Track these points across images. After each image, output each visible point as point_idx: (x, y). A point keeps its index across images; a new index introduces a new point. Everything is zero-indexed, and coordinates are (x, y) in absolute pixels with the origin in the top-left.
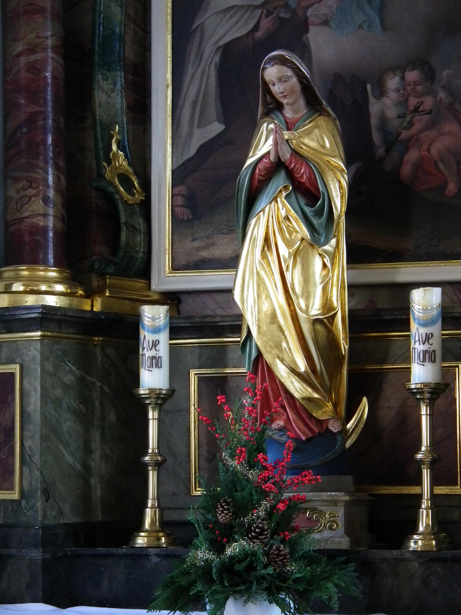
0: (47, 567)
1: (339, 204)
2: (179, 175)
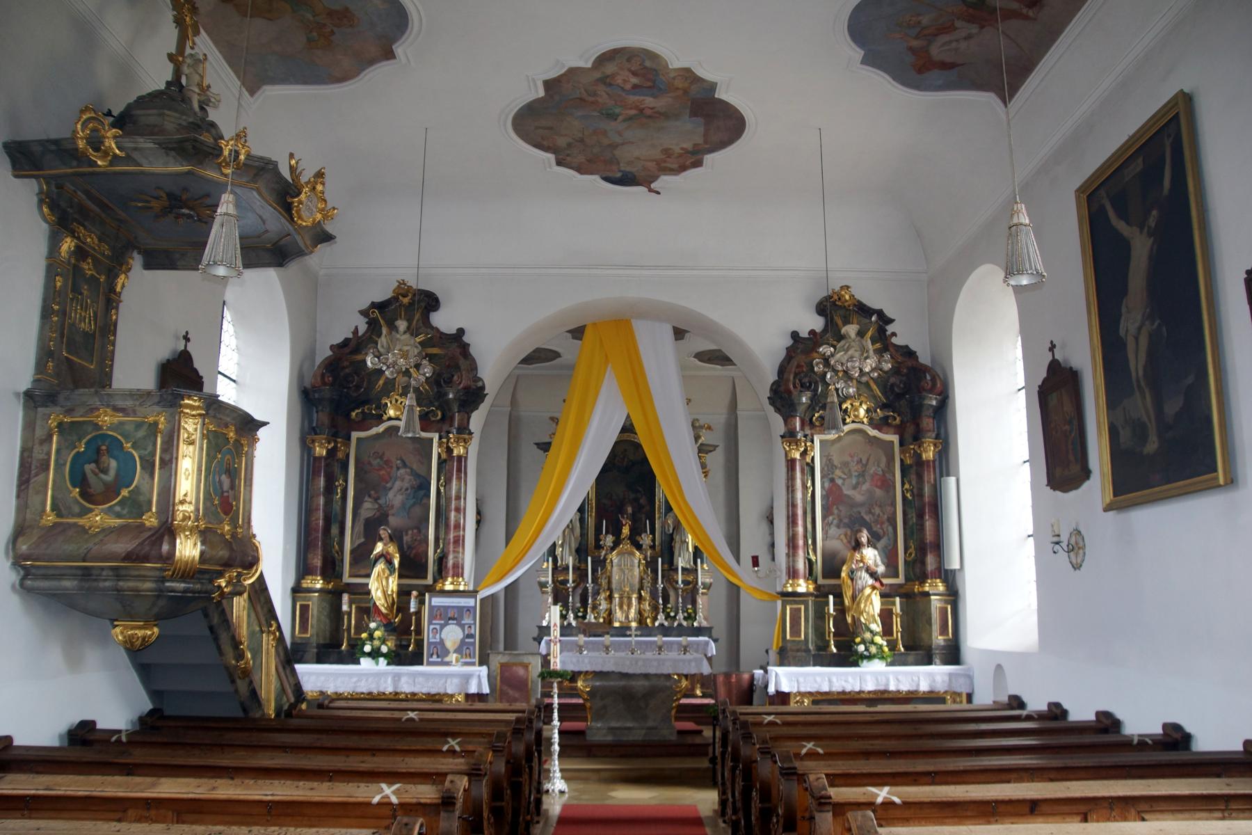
0: (318, 654)
1: (397, 565)
2: (352, 552)
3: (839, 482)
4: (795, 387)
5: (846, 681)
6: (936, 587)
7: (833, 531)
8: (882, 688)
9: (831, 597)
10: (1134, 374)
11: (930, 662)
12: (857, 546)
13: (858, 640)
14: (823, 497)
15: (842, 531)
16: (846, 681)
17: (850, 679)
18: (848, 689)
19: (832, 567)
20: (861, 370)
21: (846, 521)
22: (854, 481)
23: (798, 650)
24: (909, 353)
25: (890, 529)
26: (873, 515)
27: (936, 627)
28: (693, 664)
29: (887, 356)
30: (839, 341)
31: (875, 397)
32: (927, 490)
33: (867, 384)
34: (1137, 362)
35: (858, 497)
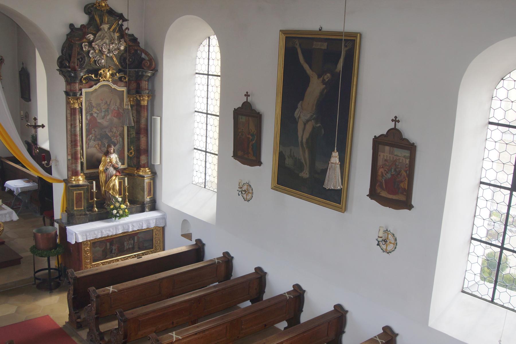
3: (95, 115)
4: (77, 65)
5: (110, 231)
6: (145, 172)
7: (92, 143)
8: (126, 231)
9: (94, 182)
10: (300, 139)
11: (143, 211)
12: (107, 153)
13: (112, 207)
14: (87, 125)
15: (96, 143)
16: (110, 231)
17: (111, 230)
18: (110, 234)
19: (94, 163)
20: (109, 50)
21: (98, 137)
22: (103, 115)
23: (81, 215)
24: (134, 40)
25: (121, 139)
26: (112, 132)
27: (146, 193)
28: (7, 216)
29: (122, 40)
30: (97, 32)
31: (115, 65)
32: (143, 121)
33: (111, 58)
34: (304, 133)
35: (105, 123)
